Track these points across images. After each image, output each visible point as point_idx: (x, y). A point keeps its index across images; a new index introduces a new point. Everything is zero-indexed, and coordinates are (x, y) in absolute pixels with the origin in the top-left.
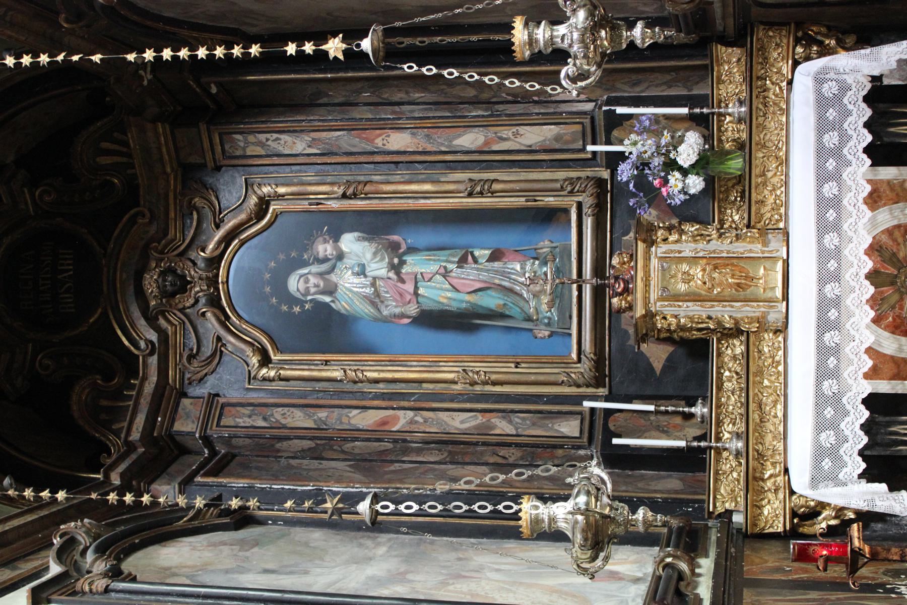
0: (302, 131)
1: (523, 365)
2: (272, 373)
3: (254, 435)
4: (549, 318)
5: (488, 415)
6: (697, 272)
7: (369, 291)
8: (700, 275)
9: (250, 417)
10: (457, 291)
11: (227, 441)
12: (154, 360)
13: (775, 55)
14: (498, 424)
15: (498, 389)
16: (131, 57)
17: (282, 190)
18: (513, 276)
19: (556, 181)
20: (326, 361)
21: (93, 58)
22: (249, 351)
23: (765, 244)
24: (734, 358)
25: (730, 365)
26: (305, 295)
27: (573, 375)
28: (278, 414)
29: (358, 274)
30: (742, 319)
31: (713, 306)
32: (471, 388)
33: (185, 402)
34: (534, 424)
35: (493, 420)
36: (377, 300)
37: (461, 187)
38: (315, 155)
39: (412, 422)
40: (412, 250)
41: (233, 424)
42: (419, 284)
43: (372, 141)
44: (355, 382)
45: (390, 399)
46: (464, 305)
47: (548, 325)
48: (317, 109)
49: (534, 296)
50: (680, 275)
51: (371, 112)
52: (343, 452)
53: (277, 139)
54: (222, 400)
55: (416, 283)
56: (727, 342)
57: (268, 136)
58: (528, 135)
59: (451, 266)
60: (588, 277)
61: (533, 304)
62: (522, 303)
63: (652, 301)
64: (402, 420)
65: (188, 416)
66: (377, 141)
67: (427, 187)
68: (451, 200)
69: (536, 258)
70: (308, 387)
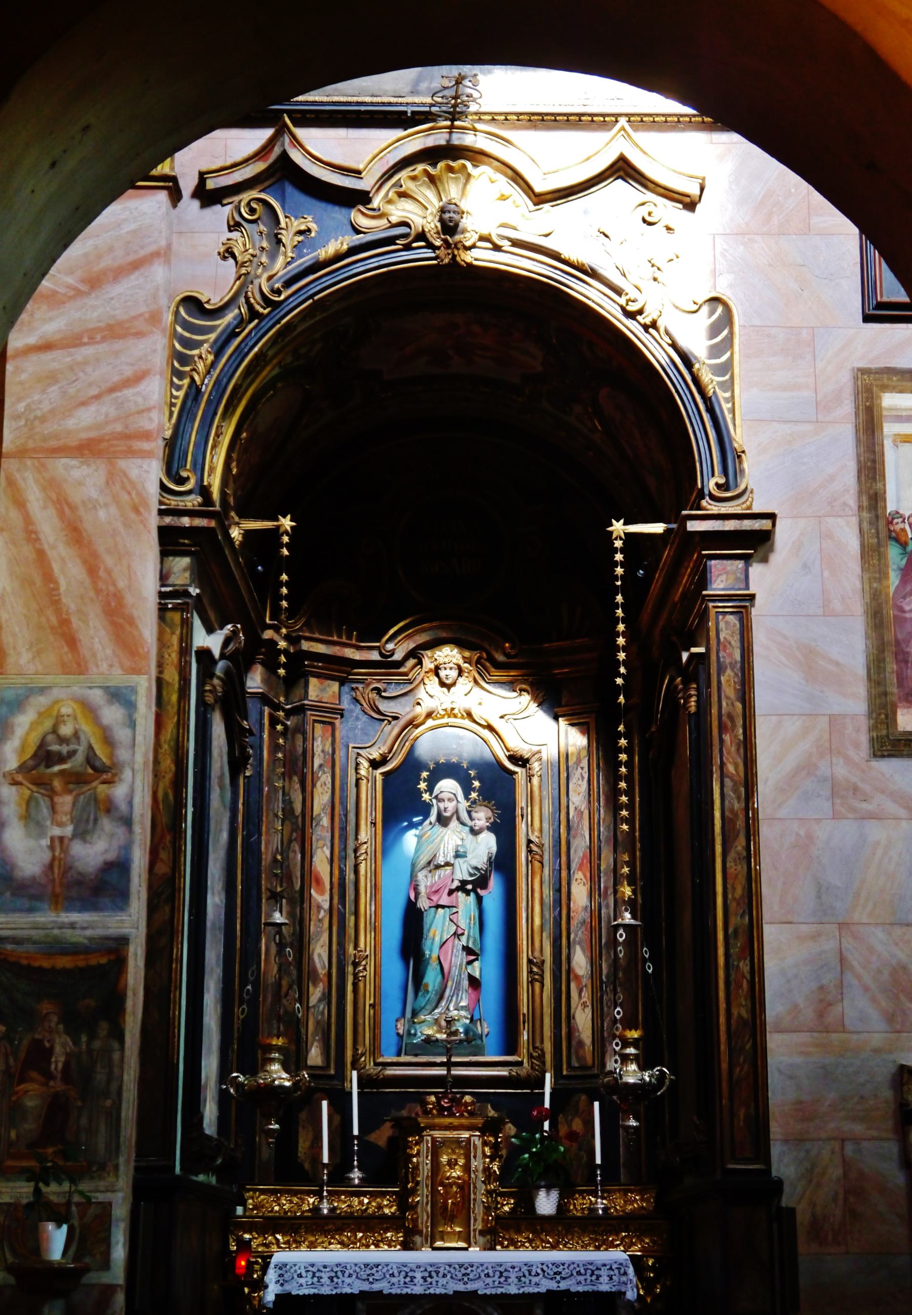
0: (589, 802)
1: (372, 1012)
2: (363, 772)
3: (306, 756)
4: (415, 1035)
5: (326, 979)
6: (457, 1173)
7: (441, 860)
8: (454, 1174)
9: (323, 751)
10: (441, 947)
11: (301, 729)
12: (375, 656)
13: (647, 1241)
14: (318, 989)
15: (350, 988)
16: (621, 728)
17: (535, 780)
18: (454, 999)
19: (542, 1042)
20: (375, 824)
21: (621, 697)
22: (384, 749)
23: (482, 1233)
24: (380, 1207)
25: (374, 1204)
26: (436, 797)
27: (363, 1059)
28: (325, 778)
29: (457, 851)
30: (416, 1213)
31: (427, 1186)
32: (350, 962)
33: (335, 686)
34: (318, 1023)
35: (321, 985)
36: (432, 866)
37: (537, 954)
38: (568, 813)
39: (319, 907)
40: (479, 899)
41: (316, 735)
42: (447, 909)
43: (580, 869)
44: (356, 851)
45: (339, 884)
46: (427, 952)
47: (409, 1033)
48: (612, 814)
49: (436, 1020)
50: (454, 1157)
51: (608, 866)
52: (290, 841)
53: (583, 778)
54: (337, 722)
55: (449, 907)
56: (394, 1201)
57: (586, 769)
58: (584, 1016)
59: (464, 939)
60: (453, 1072)
61: (428, 1018)
62: (429, 1007)
63: (432, 1132)
64: (321, 899)
65: (323, 690)
66: (580, 873)
67: (537, 921)
68: (525, 943)
69: (472, 1019)
70: (351, 806)
